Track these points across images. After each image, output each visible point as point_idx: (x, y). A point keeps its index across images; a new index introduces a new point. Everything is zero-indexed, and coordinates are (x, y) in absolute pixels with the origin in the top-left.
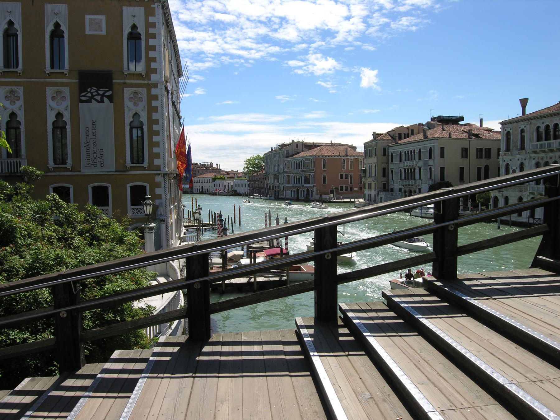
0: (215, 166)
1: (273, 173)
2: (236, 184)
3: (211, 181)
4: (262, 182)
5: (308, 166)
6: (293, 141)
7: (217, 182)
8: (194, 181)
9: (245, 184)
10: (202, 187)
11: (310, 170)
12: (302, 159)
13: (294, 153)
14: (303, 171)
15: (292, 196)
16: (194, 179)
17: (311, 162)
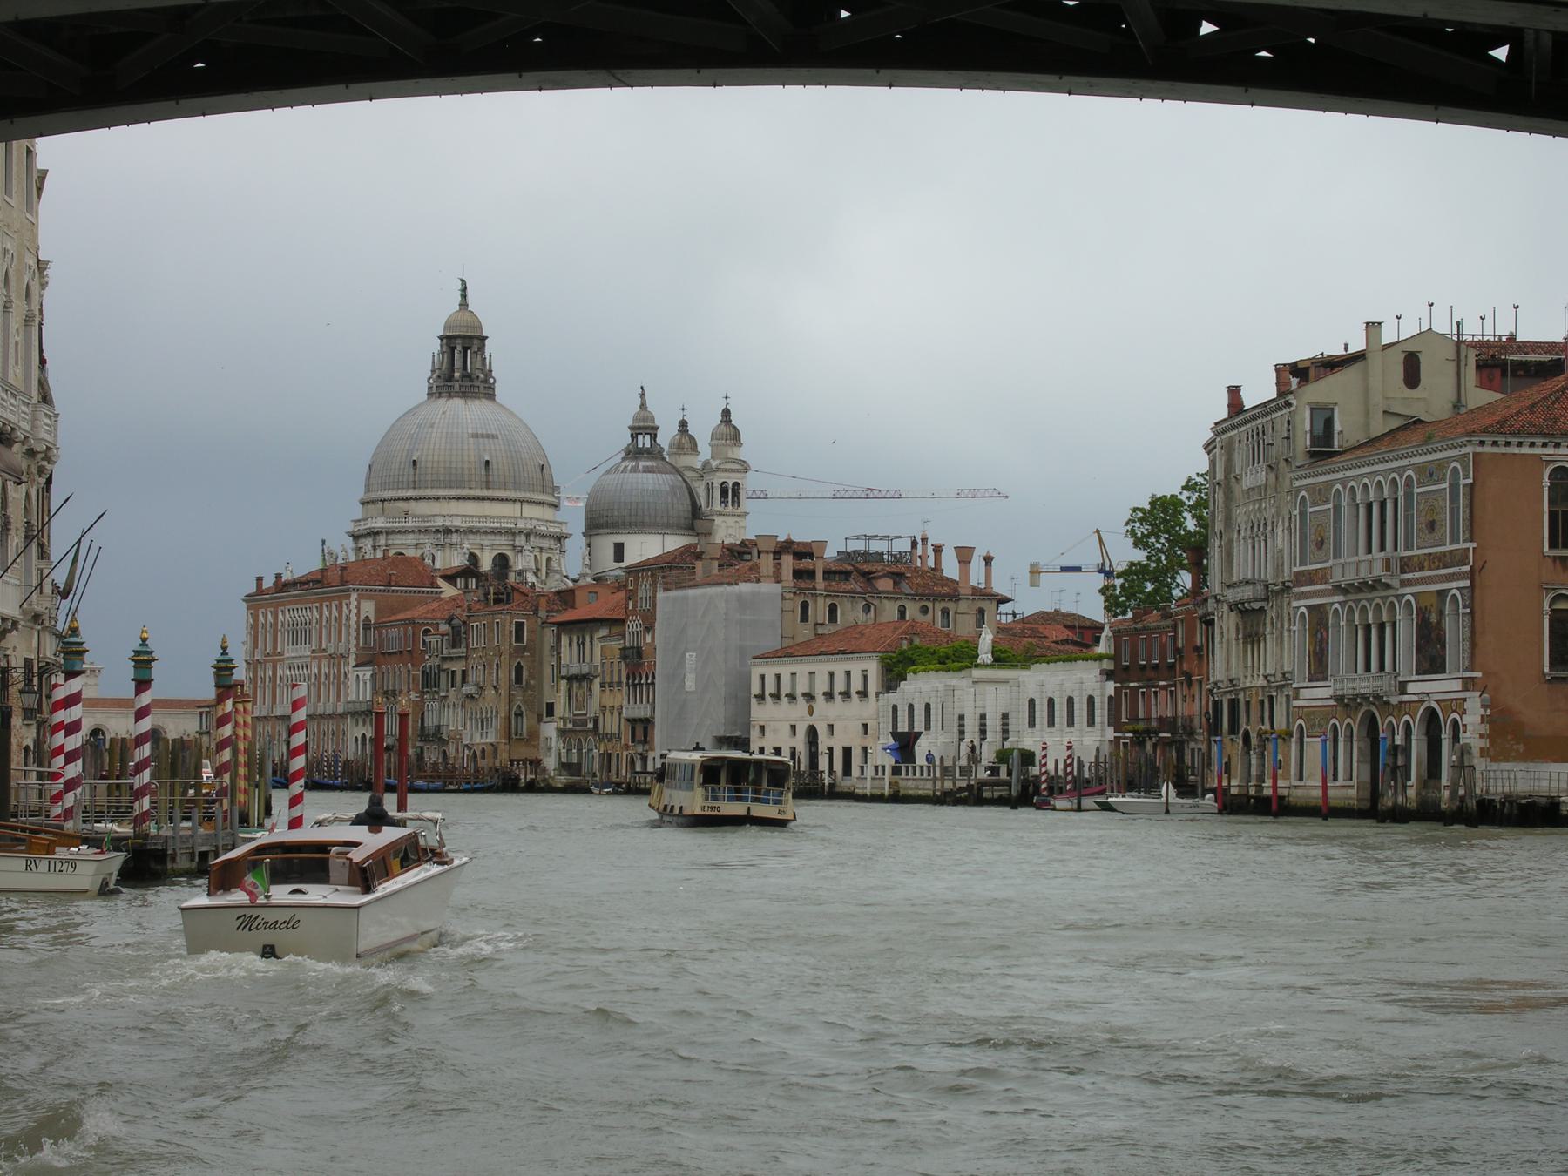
0: (951, 569)
1: (1231, 595)
2: (1032, 702)
3: (873, 687)
4: (1188, 676)
5: (1432, 526)
6: (1373, 327)
7: (921, 687)
8: (756, 690)
9: (1091, 700)
10: (812, 732)
11: (1442, 560)
12: (1405, 468)
13: (1379, 426)
14: (1406, 565)
15: (1335, 778)
16: (756, 672)
17: (1454, 487)
